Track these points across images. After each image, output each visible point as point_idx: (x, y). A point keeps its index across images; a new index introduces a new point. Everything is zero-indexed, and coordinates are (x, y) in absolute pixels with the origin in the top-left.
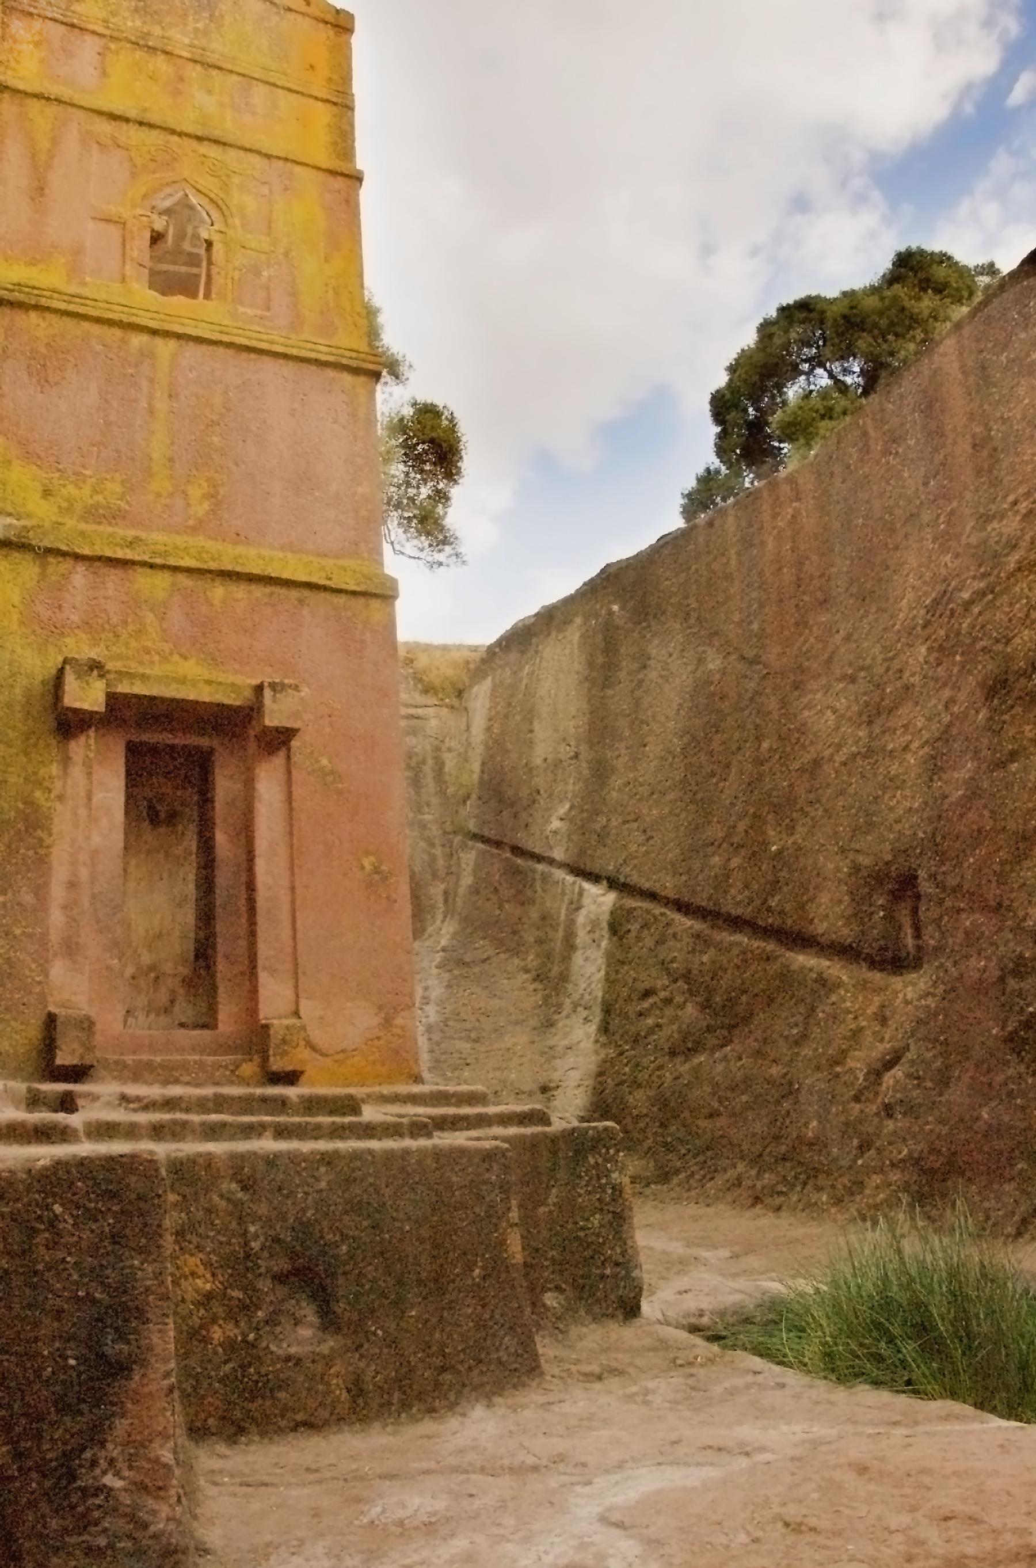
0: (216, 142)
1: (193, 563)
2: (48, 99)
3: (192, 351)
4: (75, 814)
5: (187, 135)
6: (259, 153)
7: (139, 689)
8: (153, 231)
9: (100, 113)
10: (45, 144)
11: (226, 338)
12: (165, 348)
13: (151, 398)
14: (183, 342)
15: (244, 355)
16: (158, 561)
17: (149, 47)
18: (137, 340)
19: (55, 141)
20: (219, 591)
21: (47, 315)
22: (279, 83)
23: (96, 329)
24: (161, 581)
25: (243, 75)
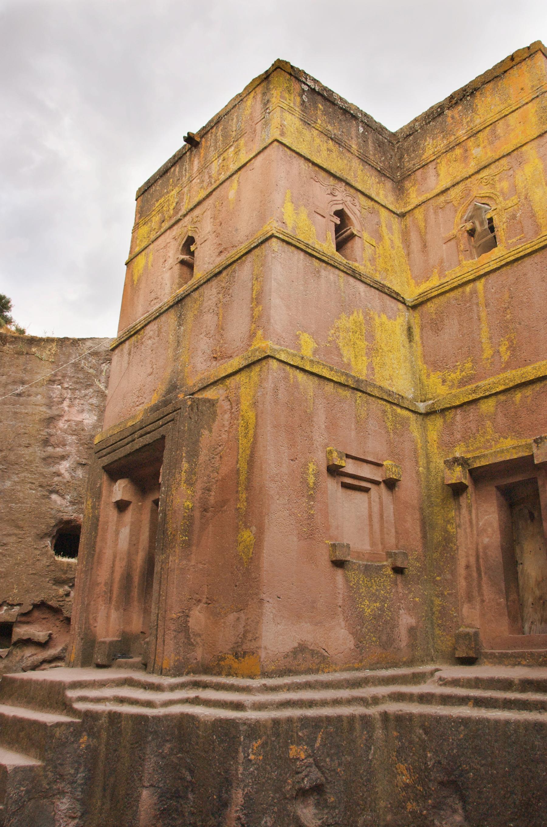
0: (485, 167)
1: (502, 388)
2: (420, 205)
3: (493, 276)
4: (465, 532)
5: (473, 175)
6: (504, 156)
7: (483, 462)
8: (468, 231)
9: (438, 195)
11: (503, 263)
12: (480, 285)
13: (478, 312)
14: (487, 276)
15: (516, 264)
16: (487, 394)
17: (451, 149)
18: (468, 289)
19: (426, 221)
20: (518, 396)
21: (433, 300)
22: (507, 113)
24: (491, 402)
25: (491, 124)
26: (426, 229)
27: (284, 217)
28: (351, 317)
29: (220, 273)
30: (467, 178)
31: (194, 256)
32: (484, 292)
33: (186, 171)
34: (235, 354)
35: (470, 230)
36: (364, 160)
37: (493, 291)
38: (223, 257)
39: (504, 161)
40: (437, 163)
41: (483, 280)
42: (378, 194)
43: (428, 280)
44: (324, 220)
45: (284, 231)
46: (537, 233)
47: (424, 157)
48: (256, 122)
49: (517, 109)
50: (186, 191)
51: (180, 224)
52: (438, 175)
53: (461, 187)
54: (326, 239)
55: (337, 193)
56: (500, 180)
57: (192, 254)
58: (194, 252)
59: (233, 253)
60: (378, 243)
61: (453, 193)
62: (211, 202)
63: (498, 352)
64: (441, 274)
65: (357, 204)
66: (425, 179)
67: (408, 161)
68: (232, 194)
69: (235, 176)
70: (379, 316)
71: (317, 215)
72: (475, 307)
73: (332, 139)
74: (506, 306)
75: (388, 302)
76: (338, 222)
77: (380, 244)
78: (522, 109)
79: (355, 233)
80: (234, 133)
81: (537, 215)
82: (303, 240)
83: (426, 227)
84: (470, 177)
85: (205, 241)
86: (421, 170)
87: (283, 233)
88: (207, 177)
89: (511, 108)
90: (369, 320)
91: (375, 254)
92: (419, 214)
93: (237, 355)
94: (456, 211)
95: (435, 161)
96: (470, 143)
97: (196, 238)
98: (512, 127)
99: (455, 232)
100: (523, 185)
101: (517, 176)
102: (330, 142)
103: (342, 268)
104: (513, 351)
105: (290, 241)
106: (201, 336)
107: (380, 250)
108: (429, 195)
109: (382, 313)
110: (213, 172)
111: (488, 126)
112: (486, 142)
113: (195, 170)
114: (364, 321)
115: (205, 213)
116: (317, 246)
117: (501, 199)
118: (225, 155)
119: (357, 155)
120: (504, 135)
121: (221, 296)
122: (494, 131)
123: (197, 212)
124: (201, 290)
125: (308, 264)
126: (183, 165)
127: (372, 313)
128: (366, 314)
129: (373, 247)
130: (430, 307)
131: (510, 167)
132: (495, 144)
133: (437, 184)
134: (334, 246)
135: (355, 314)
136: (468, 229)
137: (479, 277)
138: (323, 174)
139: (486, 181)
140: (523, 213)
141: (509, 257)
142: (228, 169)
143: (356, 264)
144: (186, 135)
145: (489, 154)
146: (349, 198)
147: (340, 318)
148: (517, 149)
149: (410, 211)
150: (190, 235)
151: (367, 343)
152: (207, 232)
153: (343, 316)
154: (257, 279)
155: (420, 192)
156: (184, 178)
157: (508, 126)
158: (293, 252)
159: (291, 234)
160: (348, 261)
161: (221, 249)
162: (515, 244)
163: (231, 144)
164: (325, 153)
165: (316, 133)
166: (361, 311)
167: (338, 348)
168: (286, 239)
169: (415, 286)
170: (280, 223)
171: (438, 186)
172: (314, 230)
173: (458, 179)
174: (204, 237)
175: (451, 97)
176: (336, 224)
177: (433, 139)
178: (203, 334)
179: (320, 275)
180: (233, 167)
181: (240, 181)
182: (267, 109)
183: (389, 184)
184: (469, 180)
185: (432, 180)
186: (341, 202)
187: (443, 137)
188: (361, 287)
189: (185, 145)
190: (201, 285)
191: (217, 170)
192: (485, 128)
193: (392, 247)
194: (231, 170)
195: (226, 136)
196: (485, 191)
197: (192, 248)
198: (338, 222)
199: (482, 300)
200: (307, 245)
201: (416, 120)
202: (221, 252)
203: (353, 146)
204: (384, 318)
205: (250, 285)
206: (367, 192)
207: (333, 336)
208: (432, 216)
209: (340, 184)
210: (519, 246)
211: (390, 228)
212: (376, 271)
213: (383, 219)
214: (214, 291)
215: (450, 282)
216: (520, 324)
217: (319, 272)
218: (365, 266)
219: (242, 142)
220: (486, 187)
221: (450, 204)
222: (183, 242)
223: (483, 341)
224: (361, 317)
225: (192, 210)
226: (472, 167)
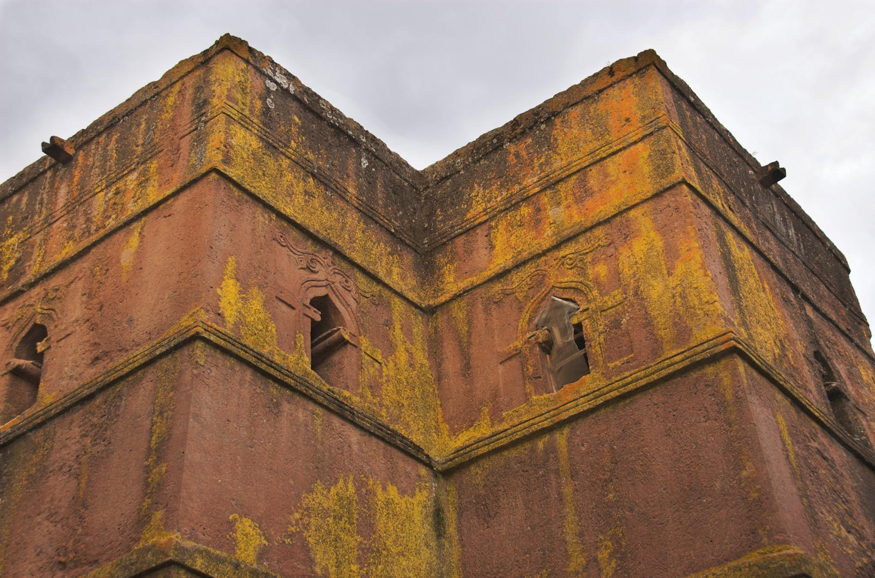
2: (460, 295)
3: (582, 427)
5: (549, 250)
6: (599, 224)
8: (539, 344)
9: (491, 280)
10: (464, 328)
11: (600, 401)
12: (561, 438)
14: (574, 424)
15: (621, 404)
17: (513, 205)
18: (540, 444)
19: (470, 323)
21: (481, 462)
22: (604, 155)
23: (513, 453)
25: (578, 171)
26: (470, 336)
27: (221, 305)
28: (332, 489)
29: (91, 397)
30: (539, 256)
31: (41, 362)
32: (569, 451)
33: (41, 203)
34: (105, 557)
35: (544, 342)
36: (368, 215)
37: (583, 449)
38: (100, 367)
39: (599, 232)
40: (491, 227)
41: (566, 431)
42: (389, 273)
43: (472, 426)
44: (294, 312)
45: (219, 328)
46: (656, 353)
47: (469, 216)
48: (181, 135)
49: (620, 150)
50: (38, 242)
51: (21, 300)
52: (492, 247)
53: (530, 269)
54: (293, 348)
55: (318, 267)
56: (594, 262)
57: (39, 358)
58: (42, 353)
59: (120, 362)
60: (386, 358)
61: (517, 279)
62: (85, 265)
63: (596, 560)
64: (496, 416)
65: (353, 288)
66: (469, 252)
67: (443, 221)
68: (127, 257)
69: (135, 225)
70: (384, 489)
71: (280, 303)
72: (552, 476)
73: (314, 176)
74: (606, 477)
75: (401, 464)
76: (318, 318)
77: (390, 358)
78: (628, 151)
79: (347, 337)
80: (140, 149)
81: (655, 322)
82: (252, 347)
83: (469, 333)
84: (544, 253)
85: (69, 335)
86: (463, 237)
87: (217, 333)
88: (82, 220)
89: (610, 148)
90: (365, 496)
91: (381, 377)
92: (458, 312)
93: (109, 560)
94: (521, 309)
95: (488, 224)
96: (545, 199)
97: (51, 328)
98: (613, 178)
99: (518, 344)
100: (632, 272)
101: (621, 258)
102: (311, 180)
103: (320, 399)
104: (621, 559)
105: (229, 347)
106: (38, 519)
107: (389, 370)
108: (475, 280)
109: (389, 483)
110: (95, 213)
111: (574, 173)
112: (571, 199)
113: (61, 205)
114: (356, 497)
115: (73, 285)
116: (277, 359)
117: (595, 292)
118: (120, 184)
119: (356, 205)
120: (600, 190)
121: (88, 441)
122: (583, 183)
123: (57, 281)
124: (49, 428)
125: (258, 391)
126: (37, 194)
127: (371, 482)
128: (360, 485)
129: (377, 365)
130: (476, 474)
131: (609, 241)
132: (586, 203)
133: (490, 261)
134: (307, 359)
135: (341, 481)
136: (540, 340)
137: (561, 425)
138: (295, 233)
139: (569, 262)
140: (632, 318)
141: (611, 391)
142: (123, 209)
143: (347, 394)
144: (48, 141)
145: (576, 218)
146: (339, 278)
147: (312, 491)
148: (620, 213)
149: (443, 304)
150: (38, 322)
151: (359, 539)
152: (73, 319)
153: (319, 487)
154: (161, 413)
155: (460, 274)
156: (36, 217)
157: (606, 175)
158: (232, 368)
159: (232, 334)
160: (331, 388)
161: (96, 353)
162: (619, 370)
163: (133, 167)
164: (300, 199)
165: (286, 163)
166: (352, 477)
167: (306, 548)
168: (222, 343)
169: (449, 436)
170: (212, 315)
171: (492, 266)
172: (274, 330)
173: (525, 255)
174: (66, 329)
175: (515, 123)
176: (313, 321)
177: (485, 188)
178: (44, 515)
179: (279, 411)
180: (133, 208)
181: (145, 233)
182: (202, 115)
183: (409, 258)
184: (543, 258)
185: (481, 254)
186: (324, 283)
187: (502, 186)
188: (354, 436)
189: (44, 159)
190: (51, 419)
191: (102, 210)
192: (569, 176)
193: (411, 365)
194: (130, 212)
195: (124, 152)
196: (569, 277)
197: (40, 347)
198: (318, 318)
199: (564, 464)
200: (259, 356)
201: (457, 154)
202: (97, 359)
203: (350, 190)
204: (393, 491)
205: (147, 423)
206: (370, 268)
207: (297, 524)
208: (481, 316)
209: (324, 252)
210: (627, 374)
211: (408, 332)
212: (381, 405)
213: (396, 316)
214: (76, 431)
215: (509, 431)
216: (631, 510)
217: (278, 405)
218: (361, 397)
219: (154, 165)
220: (570, 272)
221: (512, 297)
222: (23, 334)
223: (568, 538)
224: (351, 489)
225: (46, 276)
226: (548, 237)
